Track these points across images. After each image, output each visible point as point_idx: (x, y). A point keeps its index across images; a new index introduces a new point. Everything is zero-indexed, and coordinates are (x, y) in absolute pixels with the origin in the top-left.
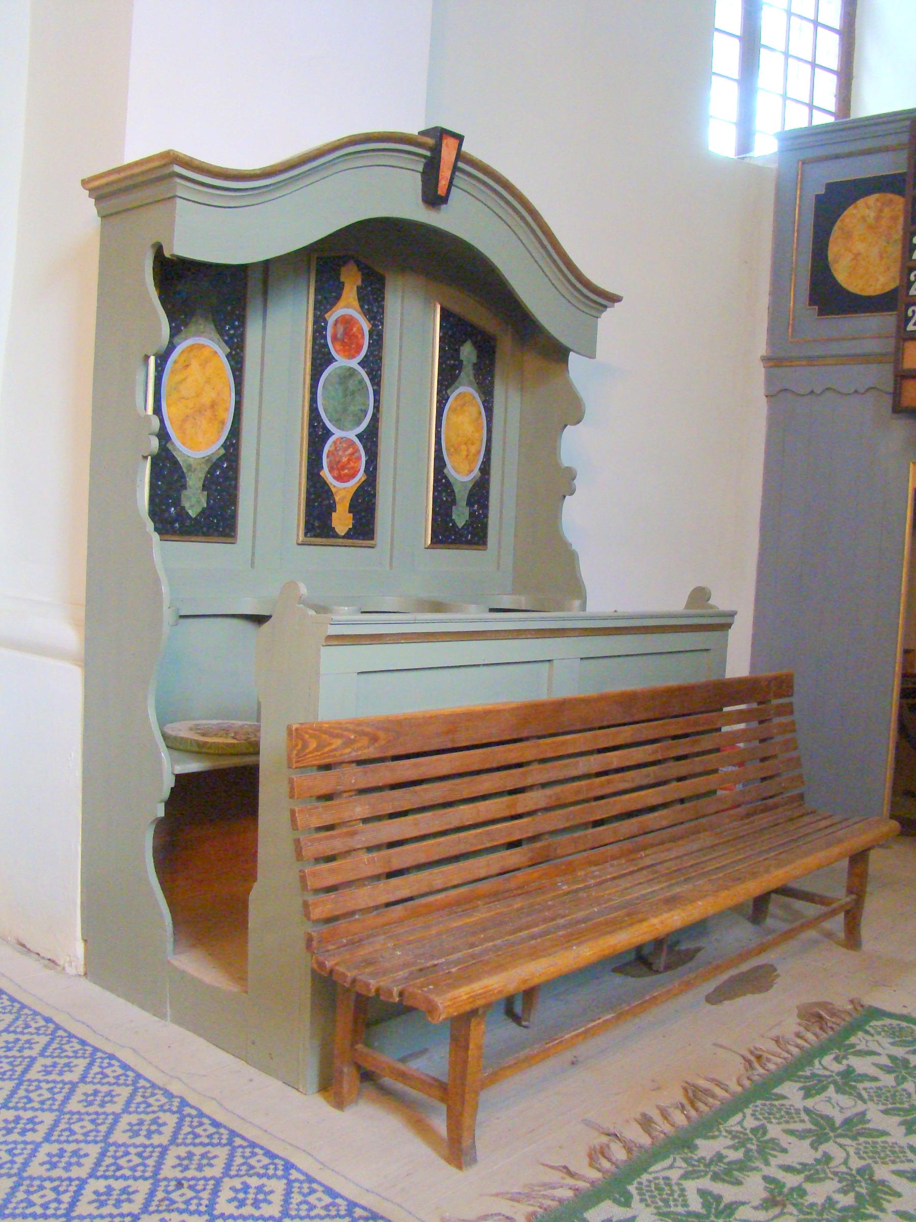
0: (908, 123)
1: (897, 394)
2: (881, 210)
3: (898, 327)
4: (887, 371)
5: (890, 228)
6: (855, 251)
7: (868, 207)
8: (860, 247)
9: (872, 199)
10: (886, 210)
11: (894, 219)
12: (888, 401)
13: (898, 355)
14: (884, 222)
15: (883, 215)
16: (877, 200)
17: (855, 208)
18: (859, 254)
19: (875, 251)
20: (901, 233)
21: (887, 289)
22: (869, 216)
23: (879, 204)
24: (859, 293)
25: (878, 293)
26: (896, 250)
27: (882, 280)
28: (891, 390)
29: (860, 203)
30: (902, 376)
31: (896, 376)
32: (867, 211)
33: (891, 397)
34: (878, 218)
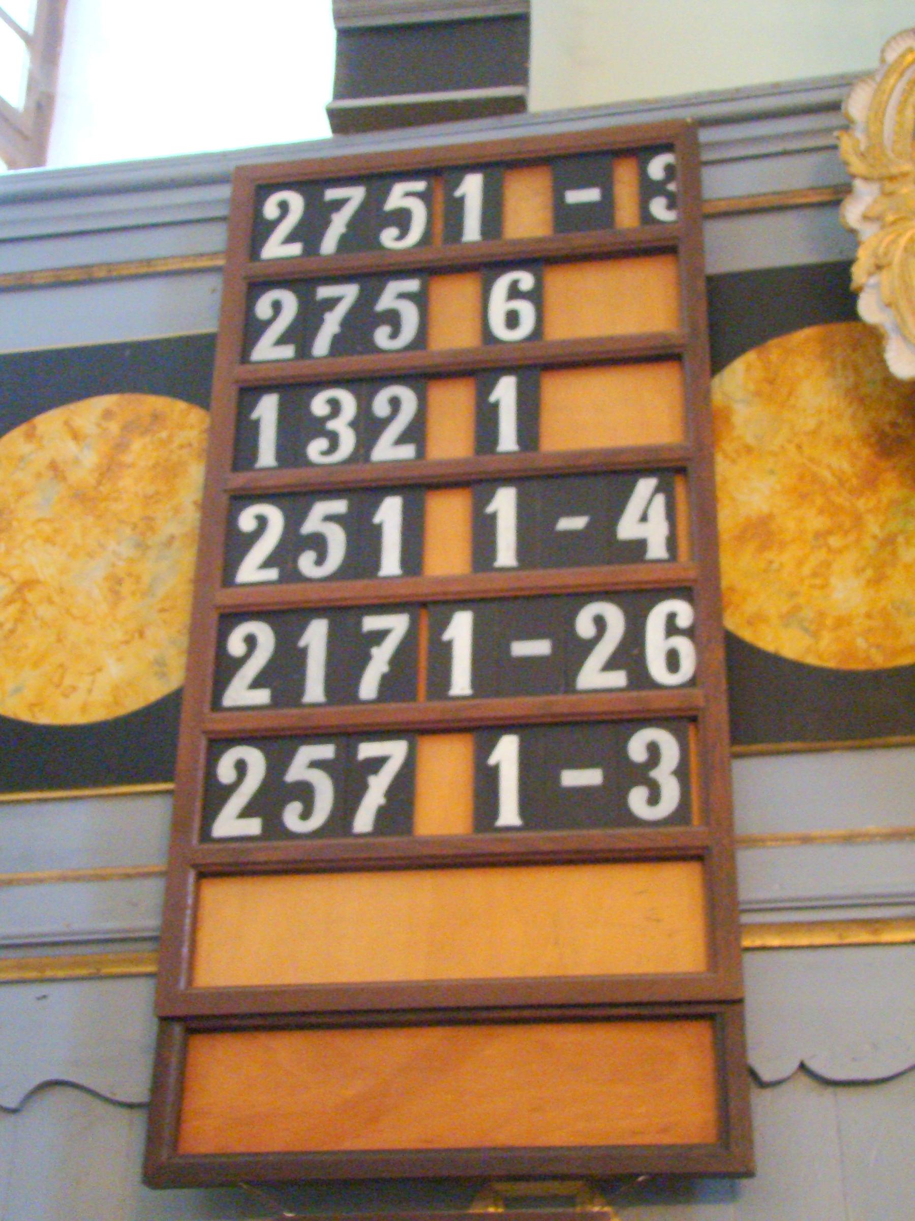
0: (225, 191)
1: (163, 1106)
2: (121, 446)
3: (179, 826)
4: (128, 1013)
5: (149, 500)
6: (17, 575)
7: (76, 436)
8: (42, 561)
9: (90, 412)
10: (140, 449)
11: (168, 472)
12: (120, 1143)
13: (172, 941)
14: (129, 483)
15: (128, 458)
16: (108, 414)
17: (30, 436)
18: (28, 584)
19: (90, 580)
20: (191, 517)
21: (133, 703)
22: (77, 461)
23: (114, 427)
24: (25, 716)
25: (98, 715)
26: (172, 572)
27: (114, 671)
28: (137, 1087)
29: (50, 422)
30: (194, 1022)
31: (165, 1020)
32: (72, 446)
33: (140, 1119)
34: (110, 468)
